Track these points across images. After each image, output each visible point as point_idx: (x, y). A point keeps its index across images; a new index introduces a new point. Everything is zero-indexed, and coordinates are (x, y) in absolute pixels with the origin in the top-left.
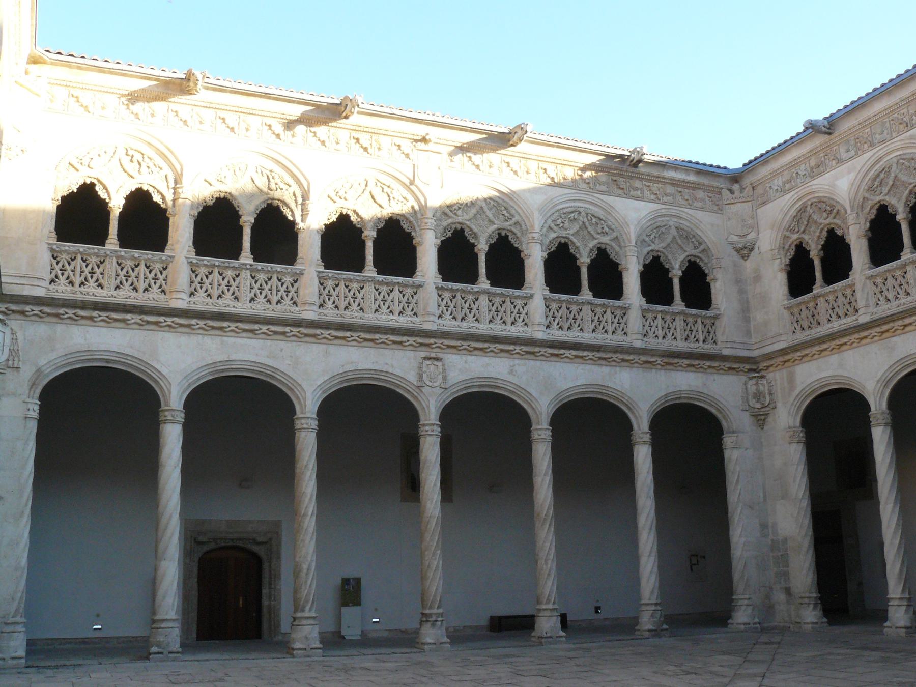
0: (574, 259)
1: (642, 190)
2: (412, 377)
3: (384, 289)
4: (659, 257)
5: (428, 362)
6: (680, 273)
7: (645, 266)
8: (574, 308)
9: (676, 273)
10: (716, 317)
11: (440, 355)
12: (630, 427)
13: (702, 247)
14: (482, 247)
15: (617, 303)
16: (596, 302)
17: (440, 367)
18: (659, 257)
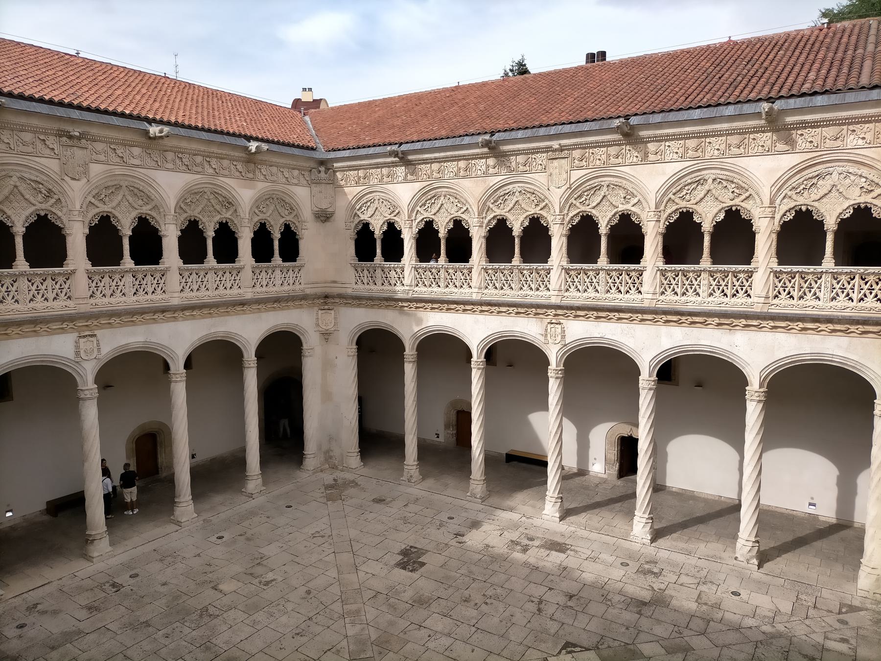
0: (201, 232)
1: (254, 172)
2: (71, 355)
3: (38, 280)
5: (85, 340)
6: (279, 236)
7: (255, 233)
8: (202, 274)
9: (277, 235)
10: (302, 266)
11: (96, 332)
12: (242, 356)
13: (295, 213)
14: (126, 230)
17: (95, 342)
18: (265, 223)
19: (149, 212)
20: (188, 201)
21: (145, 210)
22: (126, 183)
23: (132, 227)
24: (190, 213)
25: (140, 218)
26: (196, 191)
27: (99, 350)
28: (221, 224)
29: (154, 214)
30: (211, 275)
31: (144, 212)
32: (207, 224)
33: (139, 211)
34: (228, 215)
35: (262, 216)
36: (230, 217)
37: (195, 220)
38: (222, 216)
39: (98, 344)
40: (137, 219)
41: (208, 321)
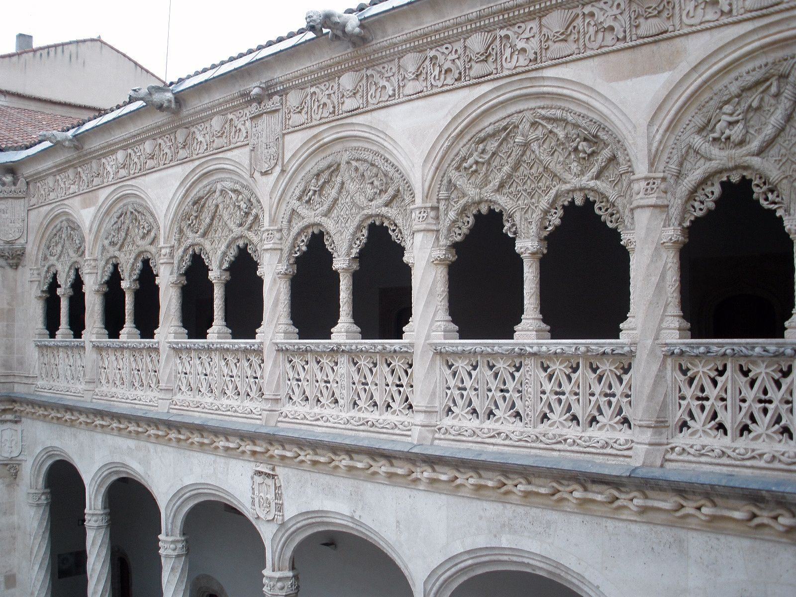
4: (745, 183)
15: (606, 344)
16: (544, 349)
18: (745, 183)
19: (384, 210)
20: (471, 161)
21: (376, 207)
22: (346, 157)
23: (355, 251)
24: (472, 193)
25: (372, 228)
26: (490, 130)
27: (280, 508)
28: (570, 210)
29: (391, 212)
30: (531, 372)
31: (374, 212)
32: (517, 218)
33: (365, 212)
34: (586, 181)
35: (720, 157)
36: (592, 184)
37: (491, 211)
38: (565, 187)
39: (278, 496)
40: (365, 232)
41: (491, 509)
